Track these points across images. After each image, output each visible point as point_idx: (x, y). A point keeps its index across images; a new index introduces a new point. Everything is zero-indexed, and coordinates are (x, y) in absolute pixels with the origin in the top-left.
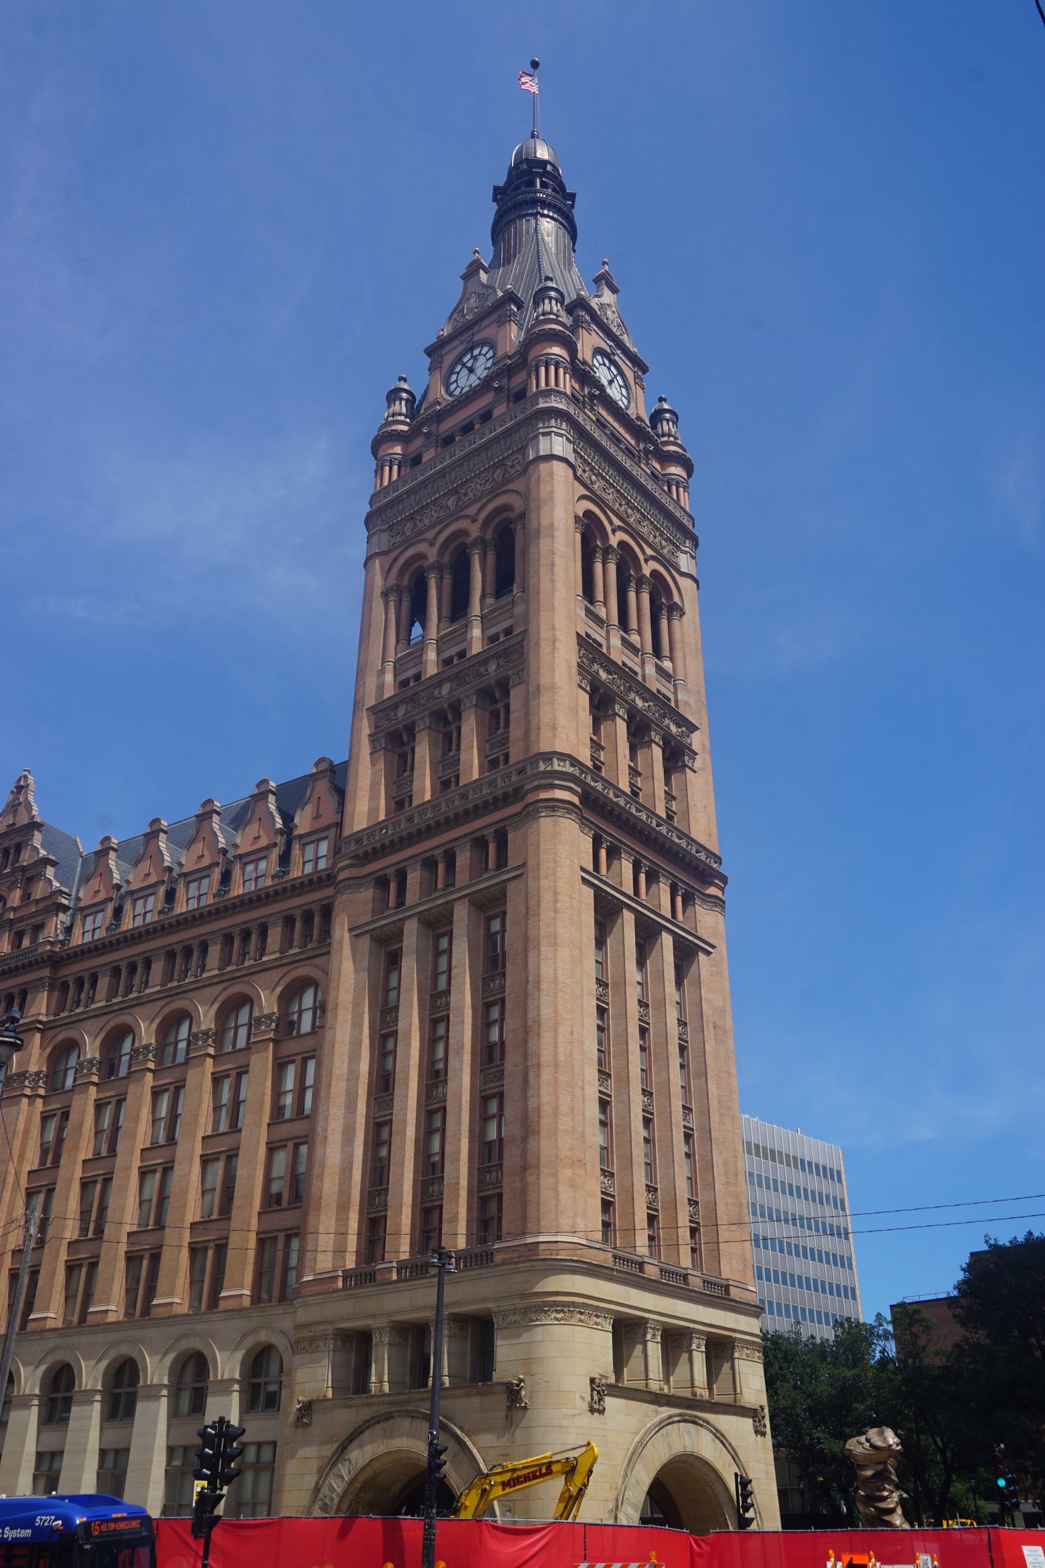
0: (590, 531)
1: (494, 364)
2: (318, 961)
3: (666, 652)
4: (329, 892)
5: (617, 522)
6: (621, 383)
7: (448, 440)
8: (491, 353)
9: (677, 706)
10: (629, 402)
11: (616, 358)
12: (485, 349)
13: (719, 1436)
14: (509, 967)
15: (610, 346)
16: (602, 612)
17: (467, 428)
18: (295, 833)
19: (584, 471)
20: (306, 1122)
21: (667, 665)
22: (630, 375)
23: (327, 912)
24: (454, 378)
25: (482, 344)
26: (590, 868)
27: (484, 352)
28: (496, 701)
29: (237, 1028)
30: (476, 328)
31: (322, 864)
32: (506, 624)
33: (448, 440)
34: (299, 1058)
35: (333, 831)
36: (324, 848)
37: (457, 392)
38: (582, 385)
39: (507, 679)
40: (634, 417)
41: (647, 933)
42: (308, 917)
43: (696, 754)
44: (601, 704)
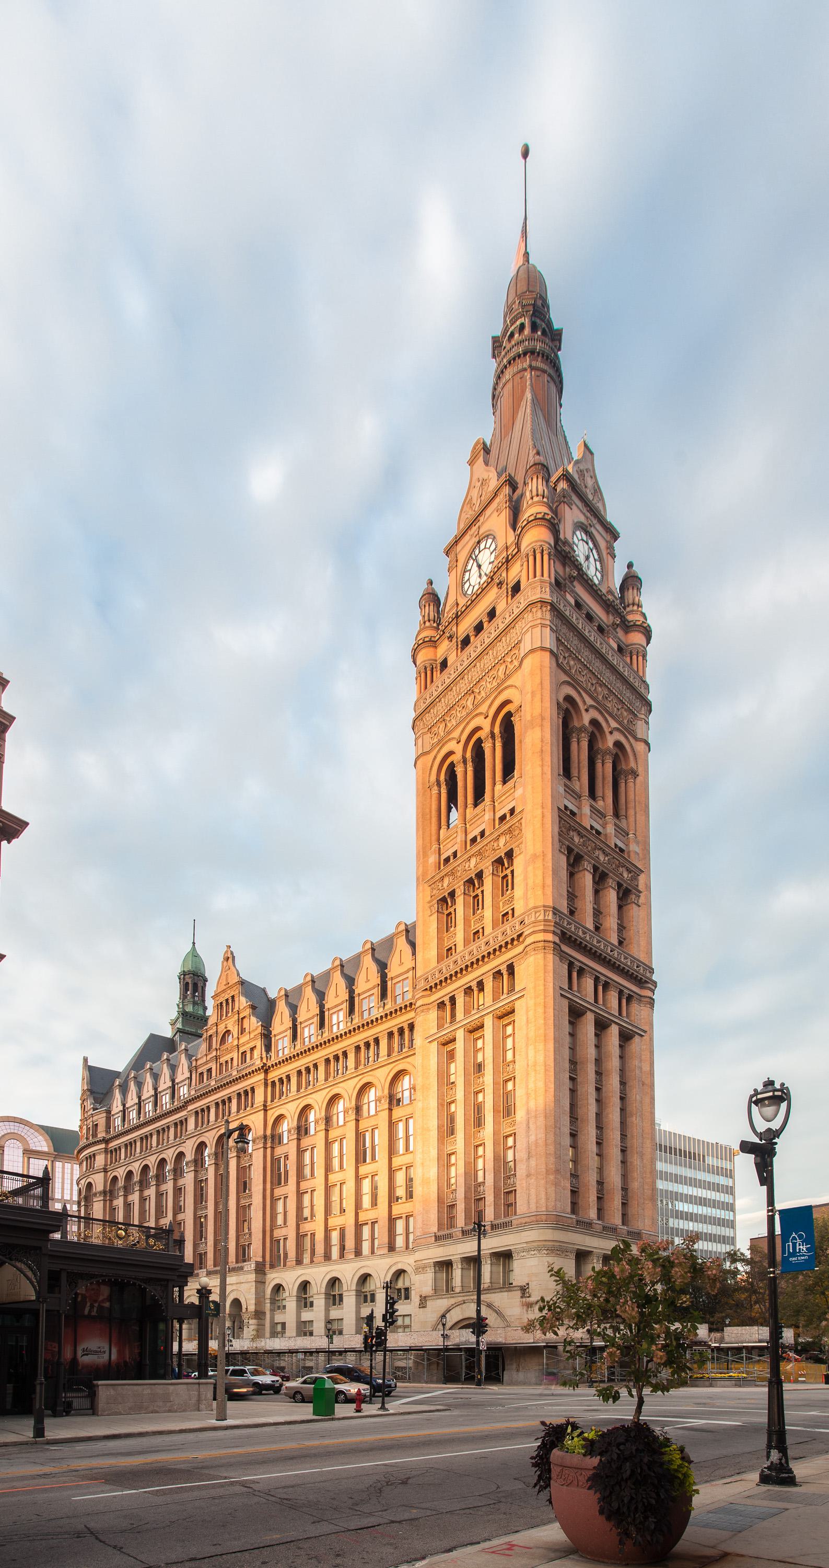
0: (567, 712)
1: (496, 558)
3: (623, 812)
5: (590, 702)
6: (596, 557)
9: (629, 857)
10: (602, 576)
11: (593, 530)
12: (490, 541)
15: (587, 518)
16: (577, 787)
19: (565, 657)
21: (623, 824)
22: (602, 544)
27: (488, 546)
30: (482, 519)
38: (564, 565)
40: (604, 591)
41: (601, 1026)
43: (640, 892)
44: (574, 860)
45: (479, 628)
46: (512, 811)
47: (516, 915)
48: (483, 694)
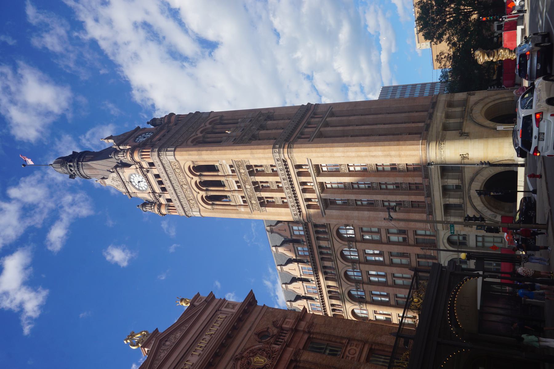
2: (332, 228)
4: (310, 224)
7: (164, 189)
8: (134, 175)
12: (132, 177)
13: (476, 103)
14: (338, 163)
17: (160, 183)
18: (290, 237)
20: (382, 230)
23: (315, 226)
24: (141, 188)
25: (130, 178)
26: (308, 139)
28: (253, 170)
29: (351, 255)
30: (124, 180)
31: (301, 228)
32: (228, 167)
33: (164, 189)
34: (362, 234)
35: (290, 225)
36: (295, 228)
37: (146, 187)
39: (247, 166)
42: (317, 232)
45: (160, 183)
46: (231, 166)
47: (274, 164)
48: (184, 180)
